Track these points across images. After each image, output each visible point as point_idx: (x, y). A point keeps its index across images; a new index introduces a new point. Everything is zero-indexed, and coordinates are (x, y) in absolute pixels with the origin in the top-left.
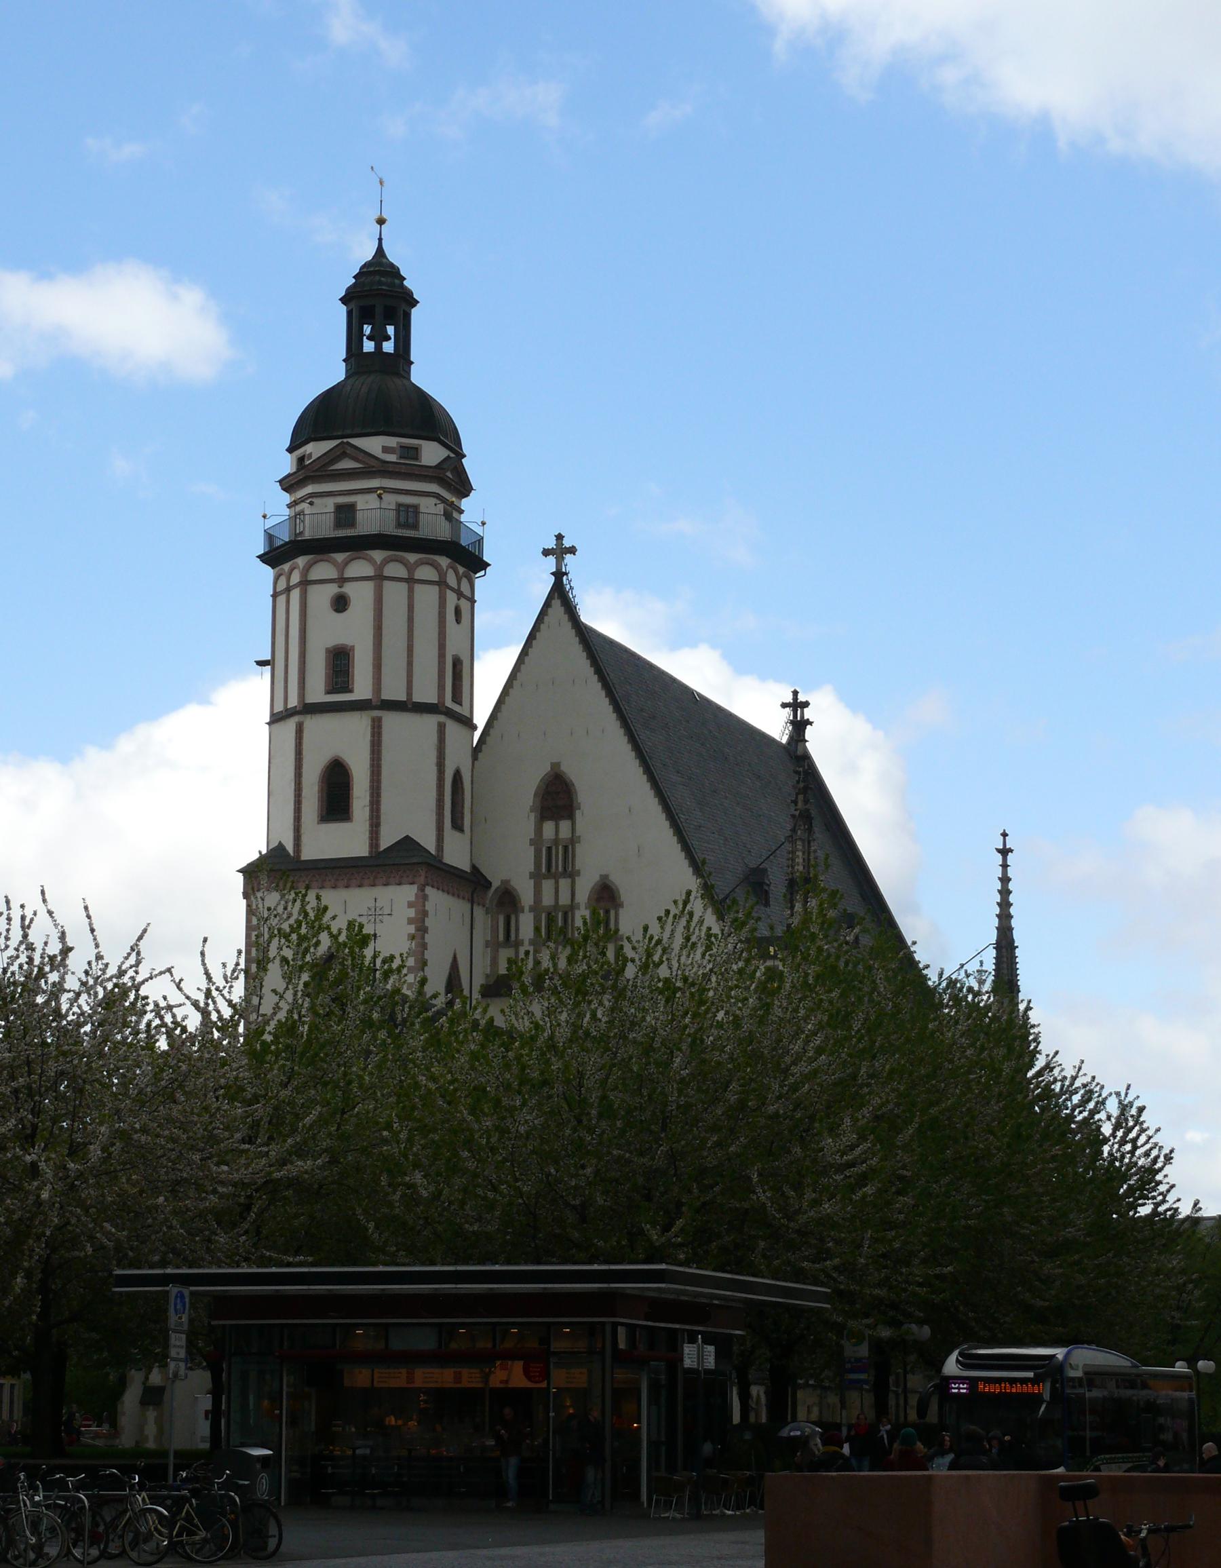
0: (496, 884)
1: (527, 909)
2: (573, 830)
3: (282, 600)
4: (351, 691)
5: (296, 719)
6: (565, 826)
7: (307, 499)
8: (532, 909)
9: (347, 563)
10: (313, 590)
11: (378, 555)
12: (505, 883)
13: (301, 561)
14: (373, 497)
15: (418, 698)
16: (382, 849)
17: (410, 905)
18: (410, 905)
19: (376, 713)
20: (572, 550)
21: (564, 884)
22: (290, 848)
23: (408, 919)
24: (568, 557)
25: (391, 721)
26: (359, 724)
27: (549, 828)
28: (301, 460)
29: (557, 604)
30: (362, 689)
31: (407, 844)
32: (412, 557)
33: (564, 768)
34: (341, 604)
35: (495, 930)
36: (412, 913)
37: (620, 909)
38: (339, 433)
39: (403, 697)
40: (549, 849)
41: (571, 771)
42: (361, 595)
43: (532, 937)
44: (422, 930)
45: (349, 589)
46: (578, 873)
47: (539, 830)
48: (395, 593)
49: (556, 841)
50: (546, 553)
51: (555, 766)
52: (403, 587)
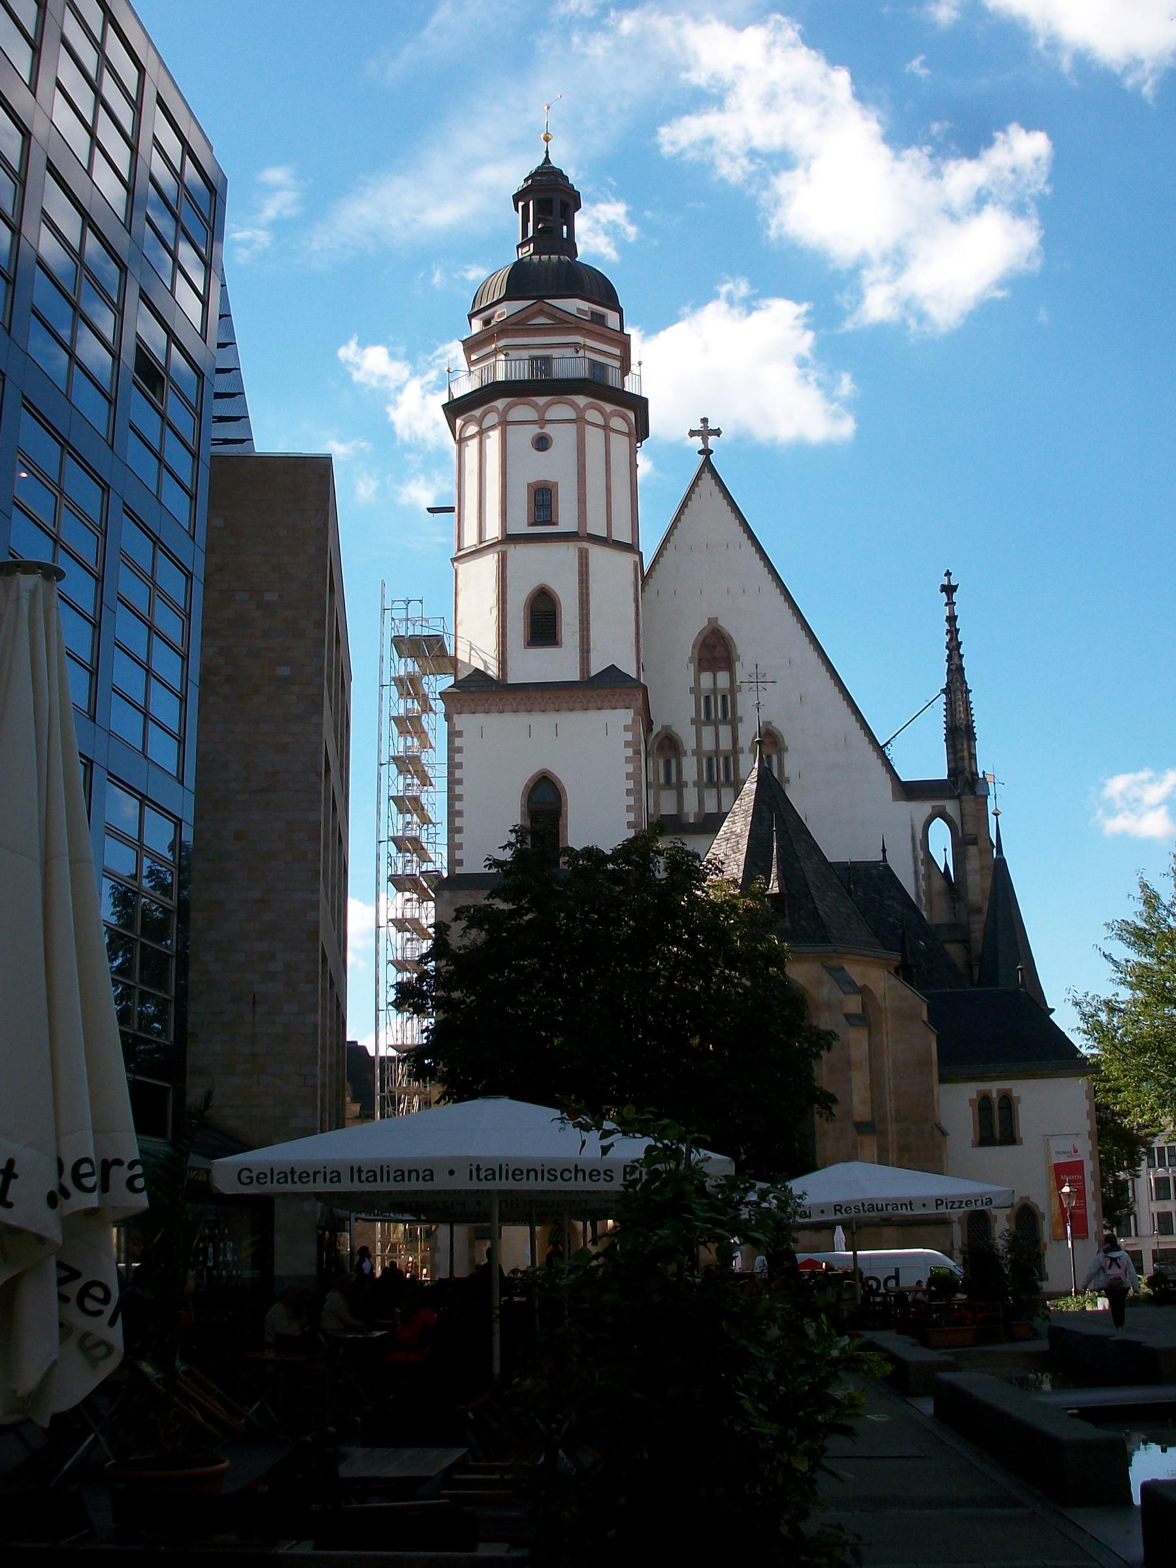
0: (657, 728)
1: (689, 752)
3: (473, 445)
4: (555, 524)
5: (499, 548)
7: (503, 350)
8: (694, 753)
9: (548, 406)
10: (511, 429)
11: (581, 400)
12: (666, 728)
13: (500, 404)
14: (569, 352)
15: (616, 536)
16: (593, 674)
17: (626, 729)
18: (626, 729)
19: (585, 545)
20: (717, 432)
21: (725, 731)
22: (493, 671)
23: (625, 742)
24: (712, 439)
25: (597, 553)
26: (567, 553)
27: (706, 679)
28: (487, 322)
29: (707, 476)
30: (566, 521)
31: (612, 672)
32: (609, 408)
33: (720, 622)
34: (542, 443)
35: (657, 773)
37: (786, 755)
38: (535, 294)
40: (707, 698)
41: (728, 625)
42: (563, 437)
43: (696, 778)
45: (549, 429)
46: (741, 719)
47: (697, 680)
48: (594, 438)
49: (715, 690)
50: (693, 433)
51: (713, 621)
52: (601, 432)
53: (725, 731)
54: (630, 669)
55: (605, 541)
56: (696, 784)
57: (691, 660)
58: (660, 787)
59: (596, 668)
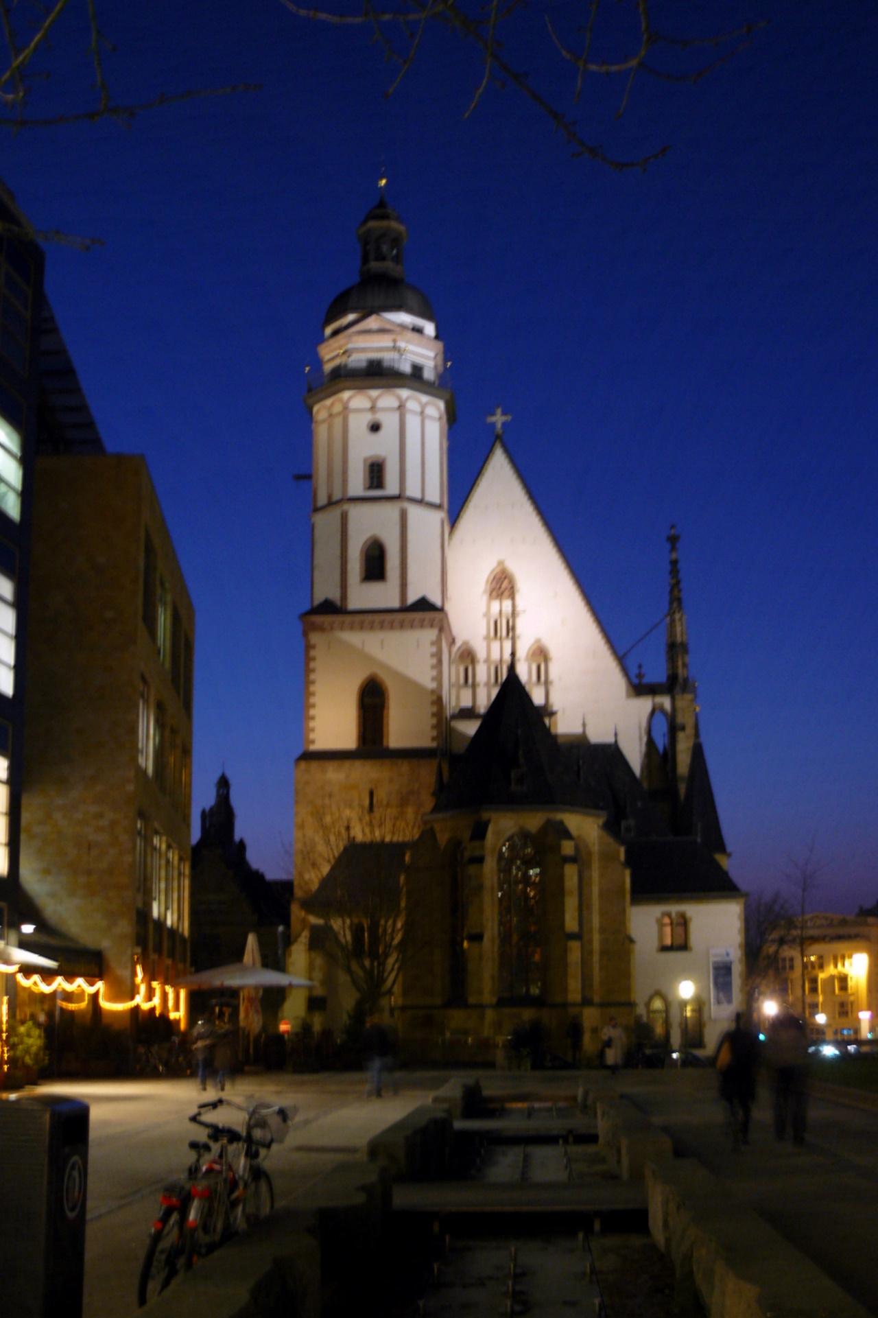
0: (458, 643)
2: (514, 606)
6: (507, 604)
18: (433, 643)
25: (414, 512)
26: (390, 512)
27: (495, 606)
30: (391, 487)
32: (424, 398)
34: (375, 428)
36: (434, 649)
39: (418, 495)
42: (390, 422)
44: (440, 662)
53: (508, 646)
54: (435, 599)
55: (420, 502)
56: (487, 684)
57: (485, 592)
58: (459, 688)
59: (412, 598)
